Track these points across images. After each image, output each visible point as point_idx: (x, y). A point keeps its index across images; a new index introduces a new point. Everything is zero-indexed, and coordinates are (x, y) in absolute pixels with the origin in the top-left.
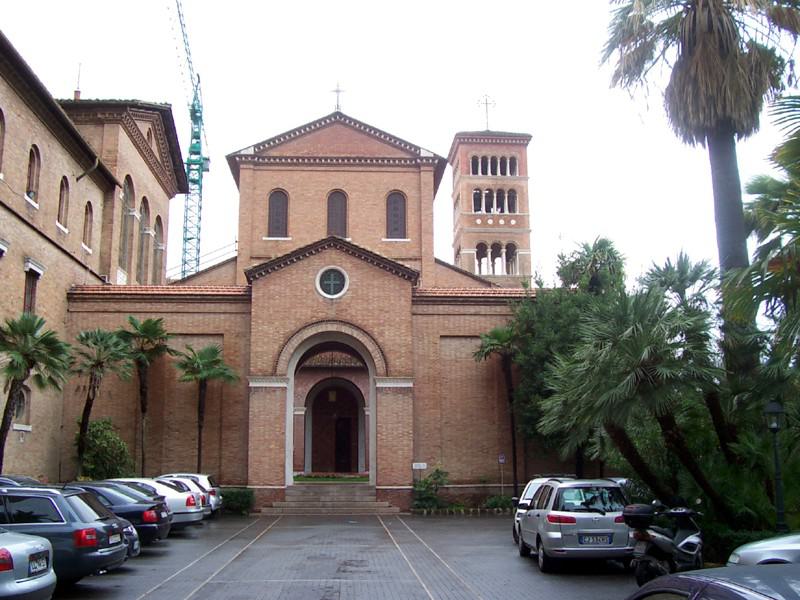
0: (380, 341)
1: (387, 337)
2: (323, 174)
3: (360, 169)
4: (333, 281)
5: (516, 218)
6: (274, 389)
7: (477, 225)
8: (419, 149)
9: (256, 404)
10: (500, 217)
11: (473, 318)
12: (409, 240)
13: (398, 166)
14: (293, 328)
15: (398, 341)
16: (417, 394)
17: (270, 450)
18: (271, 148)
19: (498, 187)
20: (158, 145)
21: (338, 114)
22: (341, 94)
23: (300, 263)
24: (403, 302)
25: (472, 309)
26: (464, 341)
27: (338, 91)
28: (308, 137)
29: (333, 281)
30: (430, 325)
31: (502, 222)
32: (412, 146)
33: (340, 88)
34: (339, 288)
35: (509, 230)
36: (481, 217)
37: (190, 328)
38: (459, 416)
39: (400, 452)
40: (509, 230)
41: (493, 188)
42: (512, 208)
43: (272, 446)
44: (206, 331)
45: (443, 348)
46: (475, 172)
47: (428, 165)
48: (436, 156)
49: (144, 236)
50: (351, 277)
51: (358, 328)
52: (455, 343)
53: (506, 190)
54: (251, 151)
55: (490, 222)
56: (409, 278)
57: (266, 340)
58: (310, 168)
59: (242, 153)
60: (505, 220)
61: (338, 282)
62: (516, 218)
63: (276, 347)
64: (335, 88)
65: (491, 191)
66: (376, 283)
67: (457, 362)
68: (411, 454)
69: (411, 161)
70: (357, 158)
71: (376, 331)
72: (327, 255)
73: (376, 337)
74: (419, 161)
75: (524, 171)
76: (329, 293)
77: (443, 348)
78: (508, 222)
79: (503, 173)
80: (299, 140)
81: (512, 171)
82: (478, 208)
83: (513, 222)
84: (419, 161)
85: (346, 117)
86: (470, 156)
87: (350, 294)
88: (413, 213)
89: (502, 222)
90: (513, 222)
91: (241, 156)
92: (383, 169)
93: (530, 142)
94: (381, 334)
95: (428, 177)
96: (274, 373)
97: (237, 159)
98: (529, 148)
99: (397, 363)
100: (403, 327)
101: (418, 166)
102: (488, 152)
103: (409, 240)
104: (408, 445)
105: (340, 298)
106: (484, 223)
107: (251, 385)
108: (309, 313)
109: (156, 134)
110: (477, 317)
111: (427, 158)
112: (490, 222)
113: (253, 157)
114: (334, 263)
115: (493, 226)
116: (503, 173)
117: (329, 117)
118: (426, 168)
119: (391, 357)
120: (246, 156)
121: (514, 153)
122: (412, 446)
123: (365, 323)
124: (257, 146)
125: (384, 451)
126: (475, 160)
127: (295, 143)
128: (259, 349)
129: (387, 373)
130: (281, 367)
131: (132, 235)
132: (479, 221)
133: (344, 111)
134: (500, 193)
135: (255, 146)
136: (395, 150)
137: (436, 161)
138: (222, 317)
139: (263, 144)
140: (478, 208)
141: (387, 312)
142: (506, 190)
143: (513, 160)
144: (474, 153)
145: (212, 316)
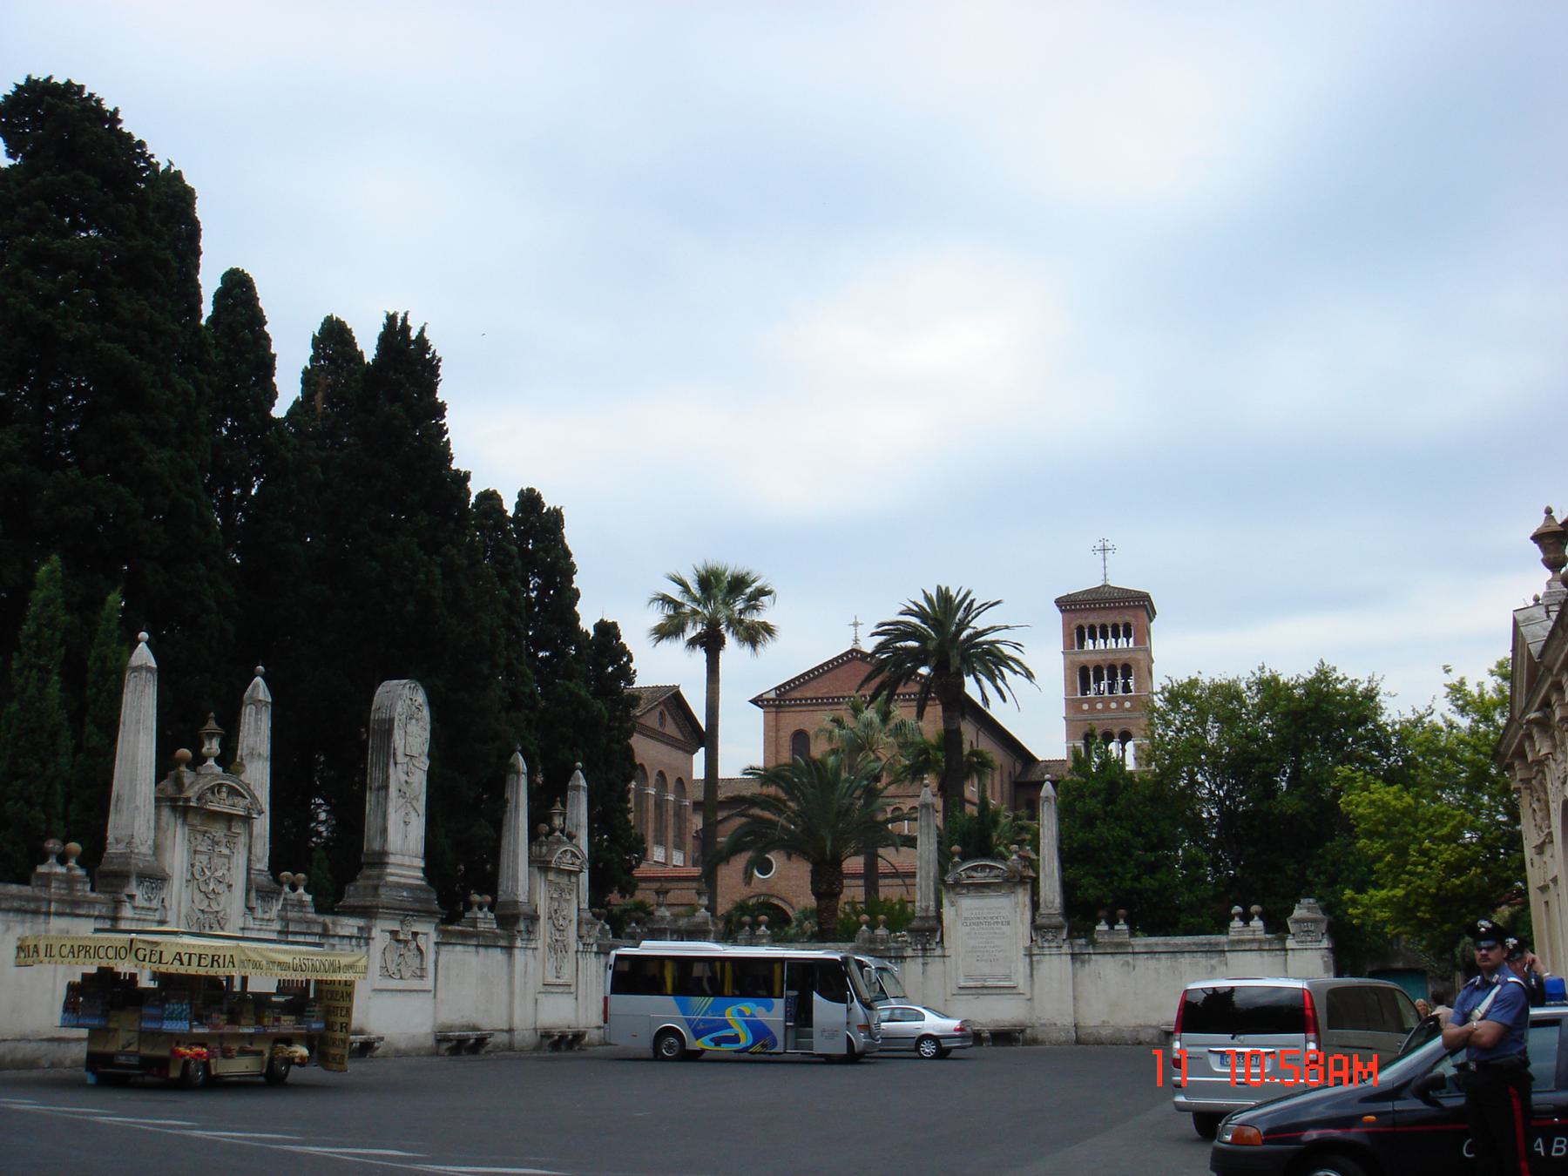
5: (1130, 699)
18: (792, 689)
27: (856, 625)
31: (1113, 705)
35: (1122, 715)
36: (1089, 701)
49: (660, 803)
54: (773, 695)
62: (1130, 699)
78: (1120, 702)
83: (1127, 705)
86: (1074, 626)
90: (1127, 705)
102: (1096, 619)
106: (1092, 708)
112: (1099, 706)
121: (1128, 619)
127: (814, 683)
132: (1085, 707)
134: (1112, 670)
139: (783, 686)
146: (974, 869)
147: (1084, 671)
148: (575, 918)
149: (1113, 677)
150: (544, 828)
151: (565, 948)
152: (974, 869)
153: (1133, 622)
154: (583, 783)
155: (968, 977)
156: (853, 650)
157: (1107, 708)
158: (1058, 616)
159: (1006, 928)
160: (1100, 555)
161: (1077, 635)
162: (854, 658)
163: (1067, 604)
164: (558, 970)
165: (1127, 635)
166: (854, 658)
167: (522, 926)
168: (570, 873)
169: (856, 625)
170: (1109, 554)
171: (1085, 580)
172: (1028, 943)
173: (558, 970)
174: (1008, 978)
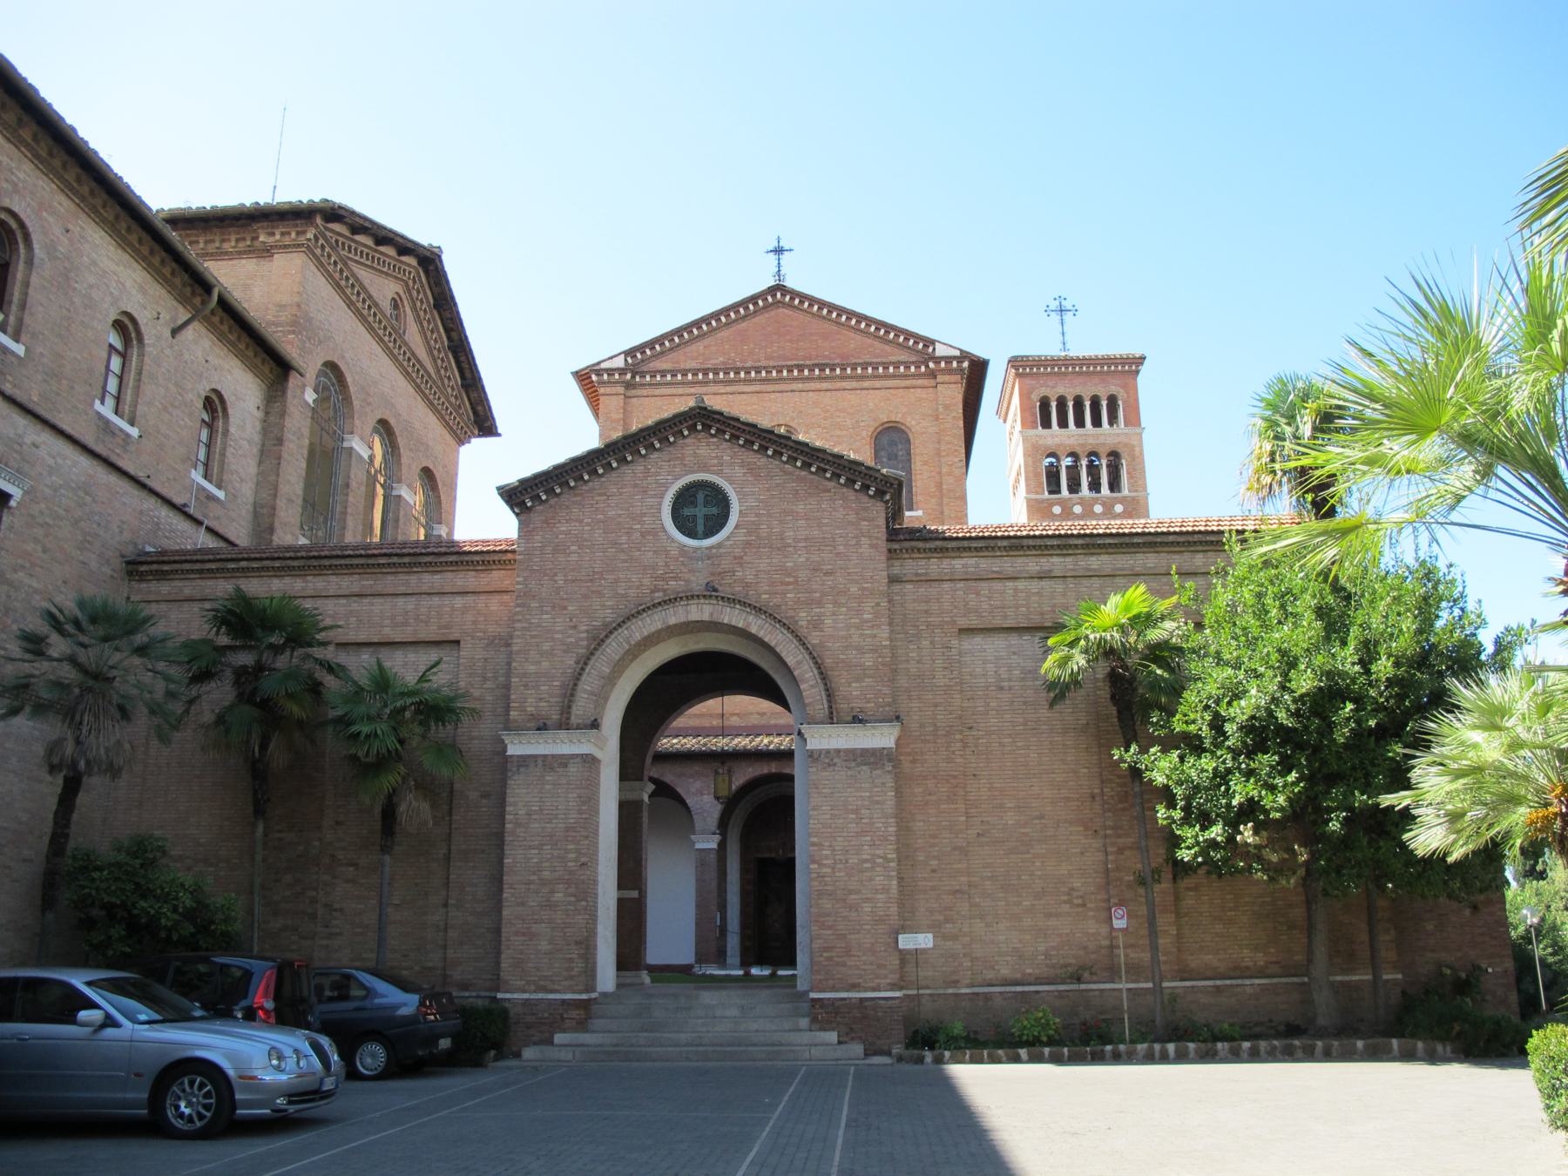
0: (814, 639)
1: (828, 631)
2: (755, 398)
3: (825, 385)
4: (701, 508)
5: (1123, 501)
6: (563, 761)
8: (933, 342)
9: (522, 796)
10: (1095, 501)
11: (1035, 586)
12: (920, 513)
13: (894, 376)
14: (609, 615)
15: (856, 639)
16: (906, 766)
17: (550, 905)
19: (1089, 449)
20: (423, 332)
21: (779, 288)
22: (785, 257)
23: (627, 470)
24: (865, 549)
25: (1033, 564)
26: (1014, 639)
27: (779, 251)
28: (725, 333)
29: (701, 508)
30: (934, 606)
32: (918, 338)
33: (785, 244)
34: (716, 523)
37: (387, 630)
38: (1010, 819)
39: (867, 908)
41: (1078, 450)
42: (1114, 485)
43: (559, 896)
44: (422, 636)
45: (967, 659)
46: (1046, 424)
47: (950, 371)
48: (965, 355)
50: (742, 497)
51: (759, 610)
52: (995, 646)
53: (1103, 452)
54: (619, 362)
55: (1077, 509)
56: (880, 494)
57: (546, 647)
58: (729, 389)
59: (603, 366)
60: (1103, 504)
61: (715, 511)
62: (1123, 501)
63: (570, 661)
64: (773, 245)
65: (1073, 454)
66: (800, 508)
67: (1002, 688)
68: (894, 909)
69: (918, 367)
70: (816, 365)
71: (803, 618)
72: (688, 451)
73: (803, 632)
74: (931, 365)
75: (1134, 420)
76: (691, 534)
77: (967, 659)
79: (1097, 422)
80: (707, 341)
81: (1113, 419)
82: (1054, 487)
84: (931, 365)
85: (795, 294)
86: (1036, 397)
87: (741, 537)
88: (925, 463)
89: (1098, 509)
90: (1119, 508)
91: (599, 373)
92: (866, 384)
93: (1144, 369)
94: (816, 624)
95: (954, 393)
96: (564, 724)
97: (594, 378)
98: (1140, 378)
99: (853, 692)
100: (868, 605)
101: (932, 374)
103: (920, 513)
104: (886, 890)
105: (719, 545)
107: (514, 749)
108: (646, 581)
110: (1043, 583)
111: (949, 360)
112: (1077, 509)
113: (622, 371)
114: (704, 468)
116: (1097, 422)
117: (762, 295)
118: (947, 378)
119: (841, 681)
120: (610, 372)
121: (1113, 390)
122: (894, 890)
123: (776, 600)
124: (630, 353)
125: (827, 904)
126: (1045, 404)
127: (699, 347)
128: (532, 668)
129: (832, 718)
130: (580, 710)
131: (347, 485)
132: (1057, 510)
133: (790, 283)
135: (627, 353)
136: (888, 348)
137: (966, 364)
138: (459, 602)
139: (641, 348)
140: (1054, 487)
141: (826, 574)
142: (1103, 452)
143: (1112, 401)
144: (1043, 392)
156: (772, 290)
160: (1055, 317)
166: (777, 304)
169: (779, 251)
170: (1068, 317)
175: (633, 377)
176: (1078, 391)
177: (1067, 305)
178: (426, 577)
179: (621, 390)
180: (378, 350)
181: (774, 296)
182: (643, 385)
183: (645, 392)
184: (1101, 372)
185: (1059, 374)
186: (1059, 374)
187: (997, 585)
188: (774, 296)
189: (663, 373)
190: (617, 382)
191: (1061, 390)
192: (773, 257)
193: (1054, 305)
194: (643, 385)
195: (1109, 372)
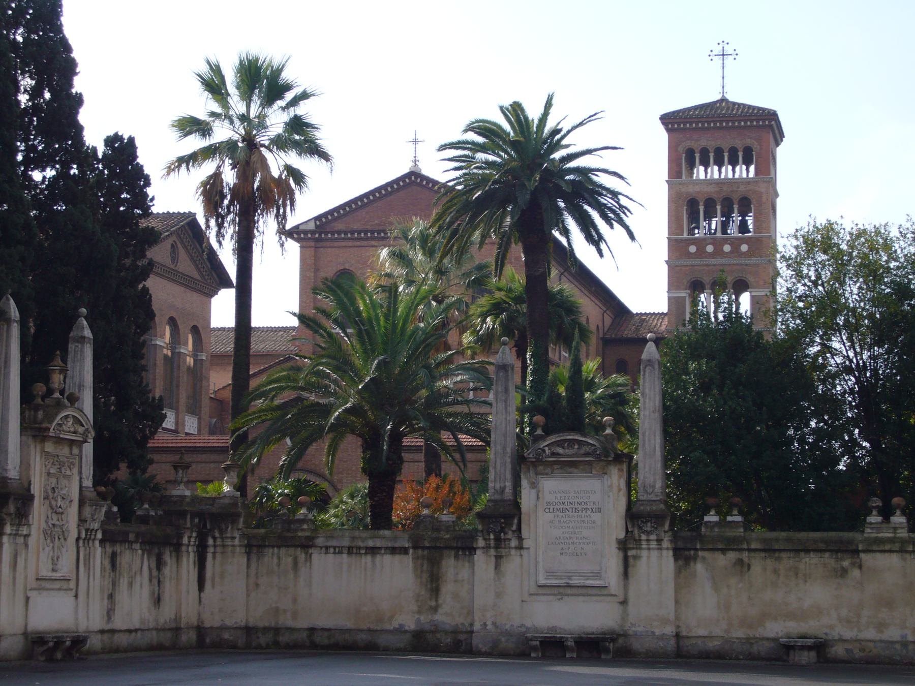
7: (689, 255)
10: (725, 241)
18: (335, 219)
22: (419, 145)
27: (415, 142)
33: (419, 137)
35: (736, 261)
36: (696, 242)
40: (736, 261)
41: (715, 196)
49: (173, 361)
53: (736, 198)
54: (311, 226)
59: (301, 228)
62: (748, 241)
64: (412, 138)
83: (744, 248)
90: (744, 248)
102: (708, 141)
109: (182, 242)
113: (313, 232)
115: (712, 255)
121: (749, 142)
132: (693, 249)
138: (212, 465)
142: (736, 198)
144: (689, 144)
145: (204, 465)
146: (559, 444)
147: (692, 204)
148: (75, 496)
149: (727, 214)
150: (40, 388)
151: (64, 536)
152: (559, 444)
153: (755, 146)
154: (88, 333)
155: (550, 573)
157: (718, 252)
158: (662, 137)
159: (596, 517)
160: (718, 61)
161: (683, 159)
162: (412, 183)
163: (671, 121)
164: (55, 561)
165: (748, 163)
167: (12, 508)
168: (72, 443)
169: (415, 142)
170: (729, 60)
171: (701, 93)
172: (622, 535)
173: (55, 561)
174: (597, 575)
175: (320, 235)
176: (719, 143)
177: (729, 49)
178: (200, 455)
179: (312, 244)
180: (165, 282)
181: (410, 179)
182: (327, 240)
183: (328, 244)
184: (740, 127)
185: (703, 129)
186: (703, 129)
187: (412, 464)
188: (410, 179)
189: (339, 233)
190: (310, 239)
191: (703, 143)
192: (412, 146)
193: (718, 50)
194: (327, 240)
195: (745, 127)
